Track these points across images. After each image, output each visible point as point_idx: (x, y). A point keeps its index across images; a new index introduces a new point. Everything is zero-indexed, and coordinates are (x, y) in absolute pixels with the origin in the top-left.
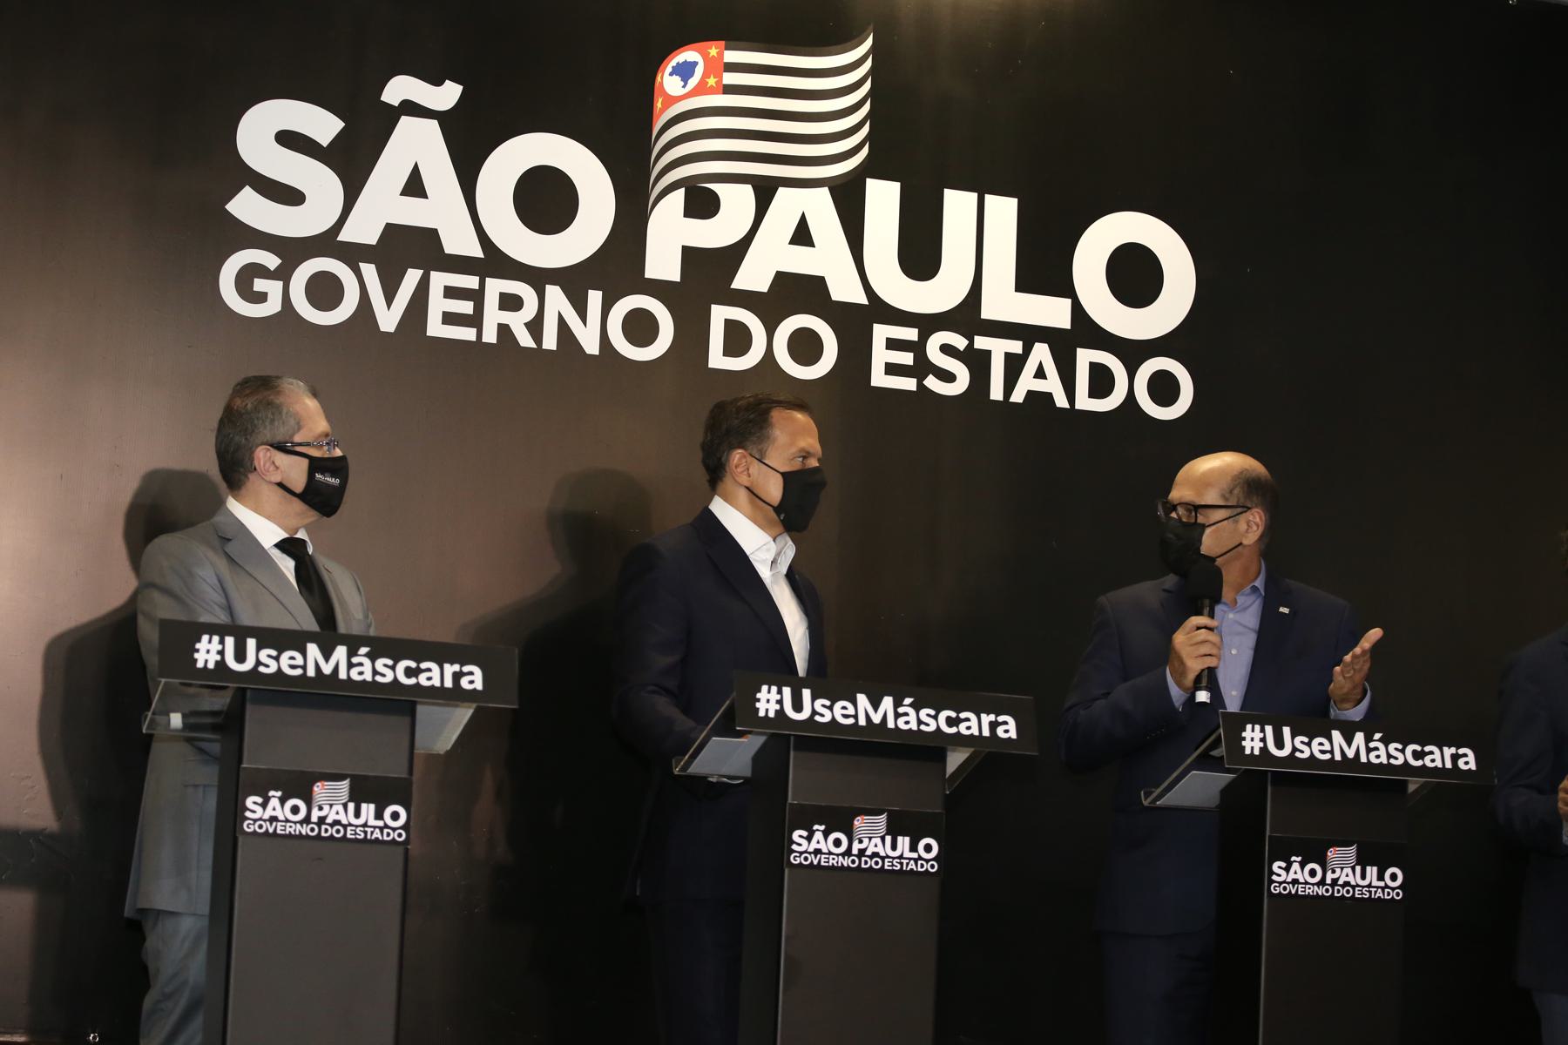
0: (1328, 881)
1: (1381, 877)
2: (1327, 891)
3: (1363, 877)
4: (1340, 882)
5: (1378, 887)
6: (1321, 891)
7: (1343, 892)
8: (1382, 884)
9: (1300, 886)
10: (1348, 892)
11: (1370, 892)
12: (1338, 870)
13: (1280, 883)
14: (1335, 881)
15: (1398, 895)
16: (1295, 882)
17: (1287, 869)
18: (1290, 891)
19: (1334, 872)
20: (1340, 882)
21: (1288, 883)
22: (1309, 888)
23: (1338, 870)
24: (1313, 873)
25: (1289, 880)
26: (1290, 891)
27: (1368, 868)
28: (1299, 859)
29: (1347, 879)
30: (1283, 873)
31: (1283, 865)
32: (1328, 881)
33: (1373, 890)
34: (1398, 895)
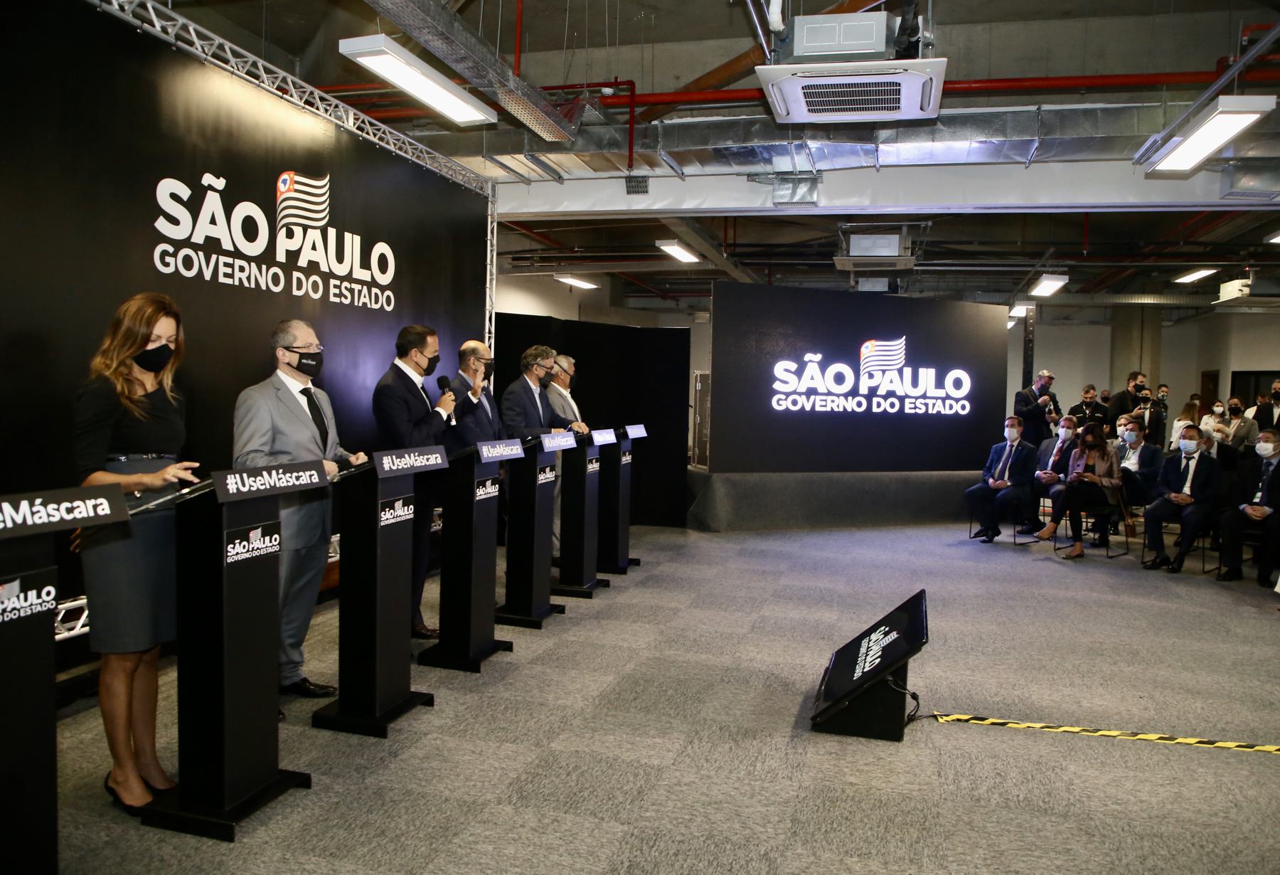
0: (863, 390)
1: (940, 383)
2: (859, 404)
3: (915, 383)
4: (881, 391)
5: (937, 398)
6: (851, 405)
7: (886, 405)
8: (941, 393)
9: (818, 398)
10: (892, 405)
11: (926, 405)
12: (878, 375)
13: (788, 395)
14: (873, 392)
15: (964, 408)
16: (811, 392)
17: (799, 373)
18: (803, 407)
19: (871, 376)
20: (881, 391)
21: (800, 394)
22: (833, 401)
23: (878, 375)
24: (839, 378)
25: (803, 389)
26: (803, 407)
27: (922, 371)
28: (819, 357)
29: (891, 388)
30: (792, 379)
31: (793, 366)
32: (863, 390)
33: (930, 402)
34: (964, 408)
